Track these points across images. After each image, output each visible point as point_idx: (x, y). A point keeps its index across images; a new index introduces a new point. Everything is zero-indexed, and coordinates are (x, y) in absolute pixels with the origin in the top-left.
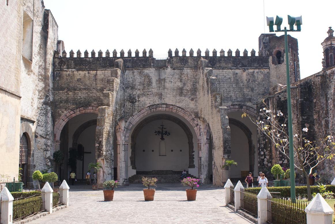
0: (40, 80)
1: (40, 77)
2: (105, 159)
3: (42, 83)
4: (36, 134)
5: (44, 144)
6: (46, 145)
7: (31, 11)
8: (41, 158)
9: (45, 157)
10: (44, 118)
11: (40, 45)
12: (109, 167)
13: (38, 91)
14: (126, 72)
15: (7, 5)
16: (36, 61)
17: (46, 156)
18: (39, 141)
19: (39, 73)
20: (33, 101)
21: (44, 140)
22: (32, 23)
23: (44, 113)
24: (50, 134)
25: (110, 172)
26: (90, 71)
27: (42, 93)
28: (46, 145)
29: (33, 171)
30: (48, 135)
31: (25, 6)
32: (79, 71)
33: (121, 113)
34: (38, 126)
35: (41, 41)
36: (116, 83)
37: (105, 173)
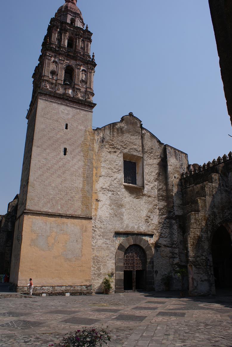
0: (161, 200)
1: (161, 198)
2: (193, 265)
3: (163, 202)
4: (159, 245)
5: (169, 252)
6: (173, 253)
7: (137, 151)
8: (167, 264)
9: (171, 263)
10: (168, 231)
11: (159, 174)
12: (202, 273)
13: (158, 209)
14: (230, 174)
15: (65, 154)
16: (151, 186)
17: (173, 262)
18: (163, 250)
19: (159, 195)
20: (149, 217)
21: (169, 249)
22: (142, 159)
23: (167, 226)
24: (177, 243)
25: (206, 278)
26: (204, 182)
27: (164, 210)
28: (173, 253)
29: (155, 276)
30: (175, 244)
31: (126, 149)
32: (197, 184)
33: (223, 216)
34: (161, 237)
35: (160, 169)
36: (209, 187)
37: (195, 280)
